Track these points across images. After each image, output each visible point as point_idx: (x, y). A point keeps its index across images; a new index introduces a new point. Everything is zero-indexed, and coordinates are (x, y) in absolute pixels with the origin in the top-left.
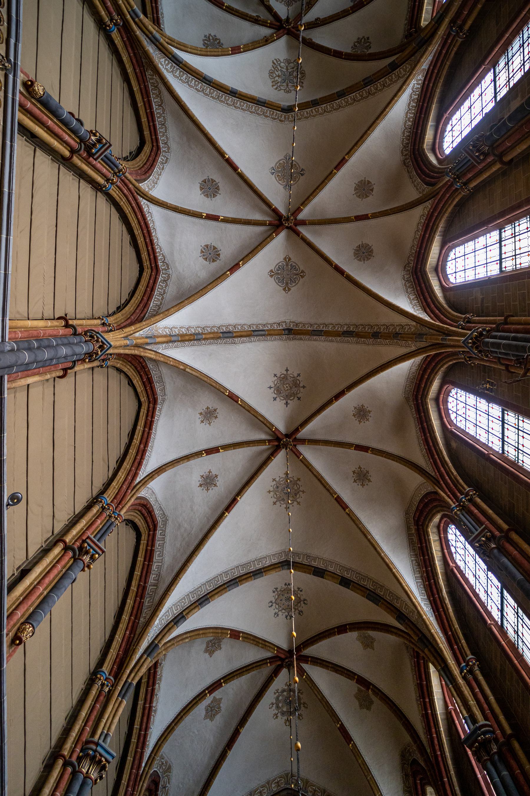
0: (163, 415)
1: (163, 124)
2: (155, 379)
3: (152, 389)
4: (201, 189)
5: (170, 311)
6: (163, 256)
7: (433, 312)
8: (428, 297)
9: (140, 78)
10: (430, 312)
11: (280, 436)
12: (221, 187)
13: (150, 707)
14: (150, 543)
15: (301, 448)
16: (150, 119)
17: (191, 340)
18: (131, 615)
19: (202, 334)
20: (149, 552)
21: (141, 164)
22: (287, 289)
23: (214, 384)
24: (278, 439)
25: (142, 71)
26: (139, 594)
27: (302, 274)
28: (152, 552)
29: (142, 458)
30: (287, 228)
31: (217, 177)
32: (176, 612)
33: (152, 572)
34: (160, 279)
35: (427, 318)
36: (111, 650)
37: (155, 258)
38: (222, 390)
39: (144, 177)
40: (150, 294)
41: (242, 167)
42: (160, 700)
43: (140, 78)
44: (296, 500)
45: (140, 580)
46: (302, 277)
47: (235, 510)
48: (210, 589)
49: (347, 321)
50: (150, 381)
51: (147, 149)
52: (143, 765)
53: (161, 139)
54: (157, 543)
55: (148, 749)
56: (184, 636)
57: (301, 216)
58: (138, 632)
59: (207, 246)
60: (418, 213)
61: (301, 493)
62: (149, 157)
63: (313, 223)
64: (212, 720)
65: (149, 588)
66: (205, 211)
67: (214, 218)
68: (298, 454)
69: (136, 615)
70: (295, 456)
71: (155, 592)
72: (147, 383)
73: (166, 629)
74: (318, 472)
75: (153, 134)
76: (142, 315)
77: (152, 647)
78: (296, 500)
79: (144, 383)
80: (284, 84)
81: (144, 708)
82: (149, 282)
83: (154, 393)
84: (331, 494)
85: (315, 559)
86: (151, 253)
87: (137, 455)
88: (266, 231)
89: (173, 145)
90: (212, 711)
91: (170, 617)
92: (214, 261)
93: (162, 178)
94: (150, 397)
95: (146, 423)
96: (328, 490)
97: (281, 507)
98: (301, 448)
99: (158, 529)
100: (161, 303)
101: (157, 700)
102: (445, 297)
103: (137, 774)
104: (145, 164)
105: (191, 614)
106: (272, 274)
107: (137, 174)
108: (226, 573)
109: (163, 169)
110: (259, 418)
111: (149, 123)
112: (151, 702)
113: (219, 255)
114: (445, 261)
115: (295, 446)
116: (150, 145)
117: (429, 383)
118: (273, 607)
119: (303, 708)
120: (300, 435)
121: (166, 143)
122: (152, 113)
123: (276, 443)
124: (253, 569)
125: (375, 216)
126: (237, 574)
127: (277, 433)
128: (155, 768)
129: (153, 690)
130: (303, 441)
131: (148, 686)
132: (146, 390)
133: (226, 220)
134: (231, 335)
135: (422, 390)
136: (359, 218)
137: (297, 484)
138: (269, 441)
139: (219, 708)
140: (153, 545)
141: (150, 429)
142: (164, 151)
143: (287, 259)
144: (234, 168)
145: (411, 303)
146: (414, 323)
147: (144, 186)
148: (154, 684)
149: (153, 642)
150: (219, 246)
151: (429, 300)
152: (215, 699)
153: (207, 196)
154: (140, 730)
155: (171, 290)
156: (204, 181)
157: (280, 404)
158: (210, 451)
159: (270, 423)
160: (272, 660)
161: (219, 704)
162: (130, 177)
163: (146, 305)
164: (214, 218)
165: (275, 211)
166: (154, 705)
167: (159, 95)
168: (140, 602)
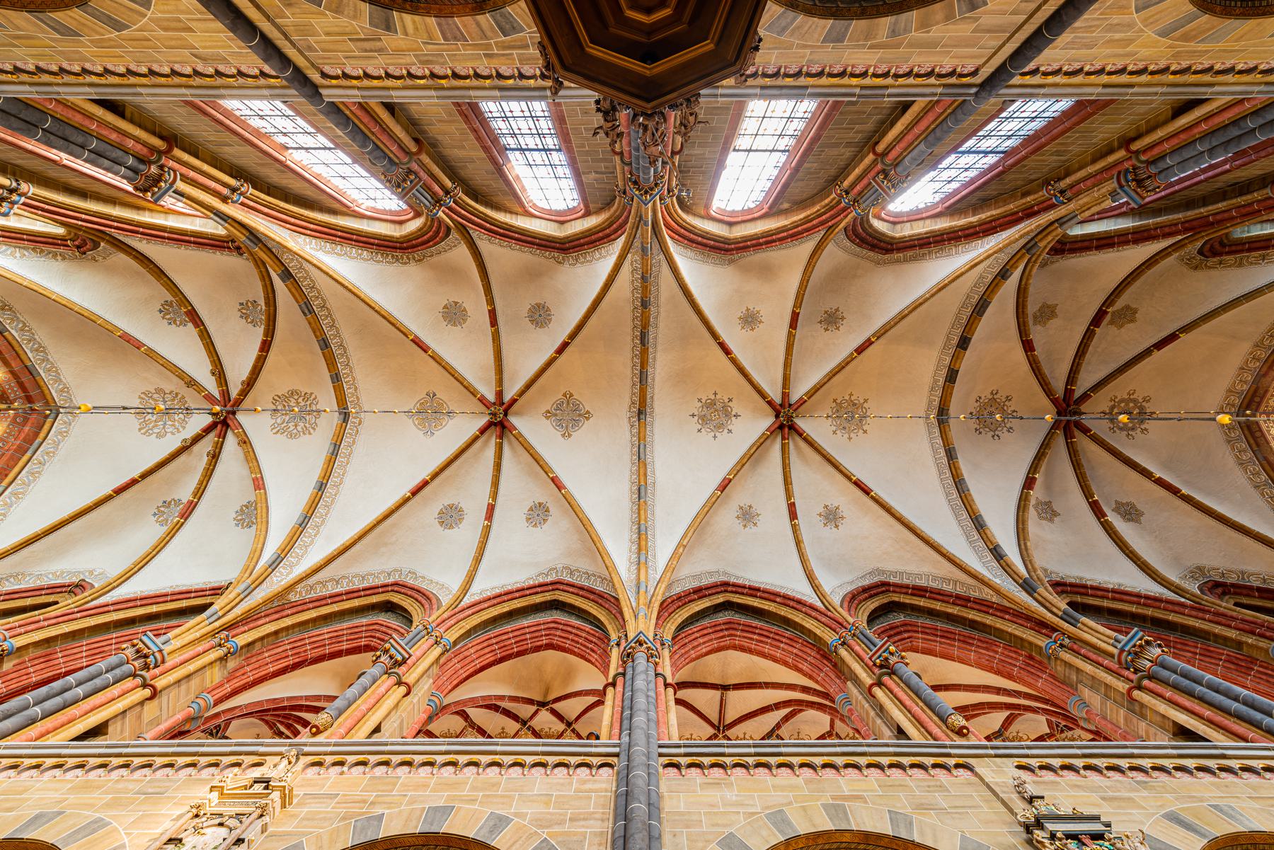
0: (743, 575)
1: (363, 578)
2: (696, 584)
3: (708, 588)
4: (451, 527)
5: (608, 564)
6: (539, 575)
7: (615, 231)
8: (596, 236)
9: (300, 608)
10: (616, 235)
11: (776, 426)
12: (450, 502)
13: (1114, 591)
14: (904, 590)
15: (794, 398)
16: (356, 595)
17: (647, 538)
18: (988, 613)
19: (639, 524)
20: (915, 592)
21: (416, 605)
22: (587, 416)
23: (706, 509)
24: (781, 427)
25: (290, 605)
26: (963, 603)
27: (568, 396)
28: (915, 588)
29: (792, 599)
30: (506, 415)
31: (437, 507)
32: (990, 557)
33: (940, 587)
34: (568, 579)
35: (623, 238)
36: (1024, 636)
37: (541, 585)
38: (714, 499)
39: (434, 601)
40: (587, 591)
41: (424, 474)
42: (1107, 579)
43: (300, 608)
44: (862, 405)
45: (947, 602)
46: (571, 395)
47: (869, 483)
48: (965, 515)
49: (629, 338)
50: (698, 591)
51: (396, 598)
52: (1183, 600)
53: (383, 580)
54: (906, 581)
55: (1163, 594)
56: (1023, 547)
57: (491, 397)
58: (1008, 604)
59: (528, 519)
60: (488, 246)
61: (853, 398)
62: (406, 595)
63: (500, 381)
64: (1142, 514)
65: (960, 590)
66: (482, 522)
67: (491, 510)
68: (802, 402)
69: (988, 606)
70: (804, 406)
71: (963, 584)
72: (701, 594)
73: (1008, 569)
74: (825, 377)
75: (376, 591)
76: (612, 600)
77: (1028, 587)
78: (862, 405)
79: (700, 598)
80: (307, 418)
81: (1114, 599)
82: (572, 593)
83: (715, 586)
84: (853, 359)
85: (935, 381)
86: (534, 590)
87: (788, 606)
88: (510, 443)
89: (389, 566)
90: (1130, 514)
91: (995, 564)
92: (547, 511)
93: (435, 578)
94: (719, 590)
95: (751, 595)
96: (848, 363)
97: (870, 424)
98: (794, 398)
99: (888, 580)
100: (600, 577)
101: (1105, 583)
102: (598, 211)
103: (1192, 608)
104: (417, 600)
105: (992, 539)
106: (567, 435)
107: (431, 609)
108: (947, 495)
109: (423, 577)
110: (752, 452)
111: (360, 597)
112: (1107, 590)
113: (540, 504)
114: (550, 212)
115: (790, 405)
116: (391, 593)
117: (706, 235)
118: (1000, 433)
119: (1135, 396)
120: (778, 400)
121: (389, 575)
122: (347, 593)
123: (786, 430)
124: (945, 460)
125: (491, 300)
126: (951, 481)
127: (773, 429)
128: (1194, 588)
129: (1093, 588)
130: (785, 395)
131: (1087, 595)
132: (710, 595)
133: (495, 494)
134: (643, 488)
135: (717, 244)
136: (494, 322)
137: (841, 403)
138: (783, 438)
139: (1127, 504)
140: (907, 587)
141: (758, 590)
142: (400, 576)
143: (548, 415)
144: (425, 484)
145: (605, 257)
146: (629, 255)
147: (446, 600)
148: (1085, 587)
149: (1021, 586)
150: (529, 504)
151: (601, 234)
152: (1116, 510)
153: (461, 520)
154: (1139, 604)
155: (584, 564)
156: (441, 523)
157: (735, 424)
158: (793, 515)
159: (760, 438)
160: (1068, 435)
161: (1123, 504)
162: (434, 617)
163: (601, 595)
164: (491, 510)
165: (483, 431)
166: (1111, 586)
167: (323, 583)
168: (974, 602)
